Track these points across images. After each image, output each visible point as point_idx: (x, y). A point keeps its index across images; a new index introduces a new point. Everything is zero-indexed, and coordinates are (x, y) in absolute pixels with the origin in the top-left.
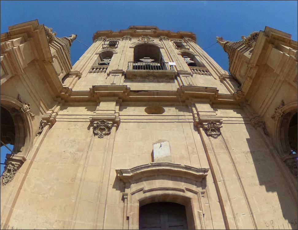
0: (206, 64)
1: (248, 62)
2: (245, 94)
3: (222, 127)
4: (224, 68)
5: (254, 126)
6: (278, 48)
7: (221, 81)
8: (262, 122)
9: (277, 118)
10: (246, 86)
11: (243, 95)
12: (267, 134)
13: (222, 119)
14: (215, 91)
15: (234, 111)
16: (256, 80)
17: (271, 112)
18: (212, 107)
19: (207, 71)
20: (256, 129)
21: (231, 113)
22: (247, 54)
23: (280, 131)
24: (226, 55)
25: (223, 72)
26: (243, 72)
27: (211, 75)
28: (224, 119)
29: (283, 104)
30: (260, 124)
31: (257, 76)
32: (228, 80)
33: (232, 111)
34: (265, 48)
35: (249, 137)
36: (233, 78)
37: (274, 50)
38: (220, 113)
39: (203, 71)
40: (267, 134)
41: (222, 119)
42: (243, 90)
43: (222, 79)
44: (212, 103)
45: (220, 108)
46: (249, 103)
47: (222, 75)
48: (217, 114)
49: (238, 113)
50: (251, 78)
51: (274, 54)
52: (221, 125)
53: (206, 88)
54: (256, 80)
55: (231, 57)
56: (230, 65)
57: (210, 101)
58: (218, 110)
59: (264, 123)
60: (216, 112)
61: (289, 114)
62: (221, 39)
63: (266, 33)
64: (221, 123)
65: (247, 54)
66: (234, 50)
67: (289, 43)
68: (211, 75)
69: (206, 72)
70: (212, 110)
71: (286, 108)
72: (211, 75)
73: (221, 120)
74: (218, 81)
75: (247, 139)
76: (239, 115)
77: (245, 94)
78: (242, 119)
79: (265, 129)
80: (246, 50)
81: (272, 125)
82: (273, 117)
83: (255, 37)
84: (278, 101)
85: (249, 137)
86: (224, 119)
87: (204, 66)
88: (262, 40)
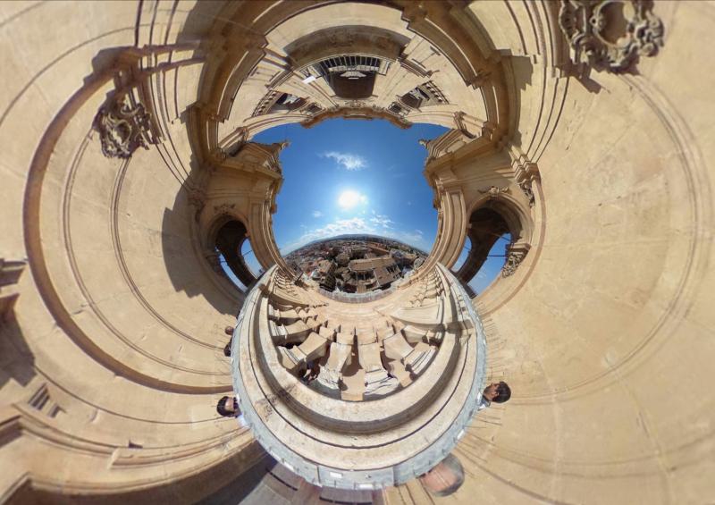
0: (270, 116)
1: (259, 164)
2: (223, 165)
3: (147, 148)
4: (256, 136)
5: (189, 199)
6: (271, 187)
7: (239, 129)
8: (202, 203)
9: (218, 212)
10: (232, 163)
11: (221, 162)
12: (197, 219)
13: (165, 140)
14: (224, 116)
15: (192, 157)
16: (241, 173)
17: (219, 203)
18: (189, 109)
19: (261, 113)
20: (189, 204)
21: (186, 153)
22: (266, 163)
23: (212, 226)
24: (270, 142)
25: (252, 134)
26: (249, 158)
27: (253, 116)
28: (167, 143)
29: (233, 206)
30: (199, 203)
31: (246, 174)
32: (240, 138)
33: (190, 153)
34: (270, 178)
35: (171, 208)
36: (242, 146)
37: (269, 185)
38: (177, 131)
39: (263, 107)
40: (197, 219)
41: (165, 140)
42: (227, 160)
43: (242, 131)
44: (198, 109)
45: (188, 127)
46: (213, 173)
47: (247, 131)
48: (175, 125)
49: (191, 164)
50: (243, 167)
51: (267, 184)
52: (150, 143)
53: (232, 100)
54: (241, 173)
55: (267, 148)
56: (259, 145)
57: (204, 105)
58: (184, 124)
59: (203, 206)
60: (179, 121)
61: (230, 216)
62: (287, 145)
63: (280, 179)
64: (155, 142)
65: (266, 163)
66: (273, 152)
67: (275, 193)
68: (253, 116)
69: (260, 111)
70: (182, 109)
71: (232, 212)
72: (253, 115)
73: (161, 139)
74: (240, 124)
75: (167, 210)
76: (189, 169)
77: (223, 165)
78: (185, 177)
79: (199, 212)
80: (270, 163)
81: (209, 215)
82: (216, 208)
83: (279, 171)
84: (232, 201)
85: (171, 208)
86: (167, 143)
87: (269, 112)
88: (276, 176)
